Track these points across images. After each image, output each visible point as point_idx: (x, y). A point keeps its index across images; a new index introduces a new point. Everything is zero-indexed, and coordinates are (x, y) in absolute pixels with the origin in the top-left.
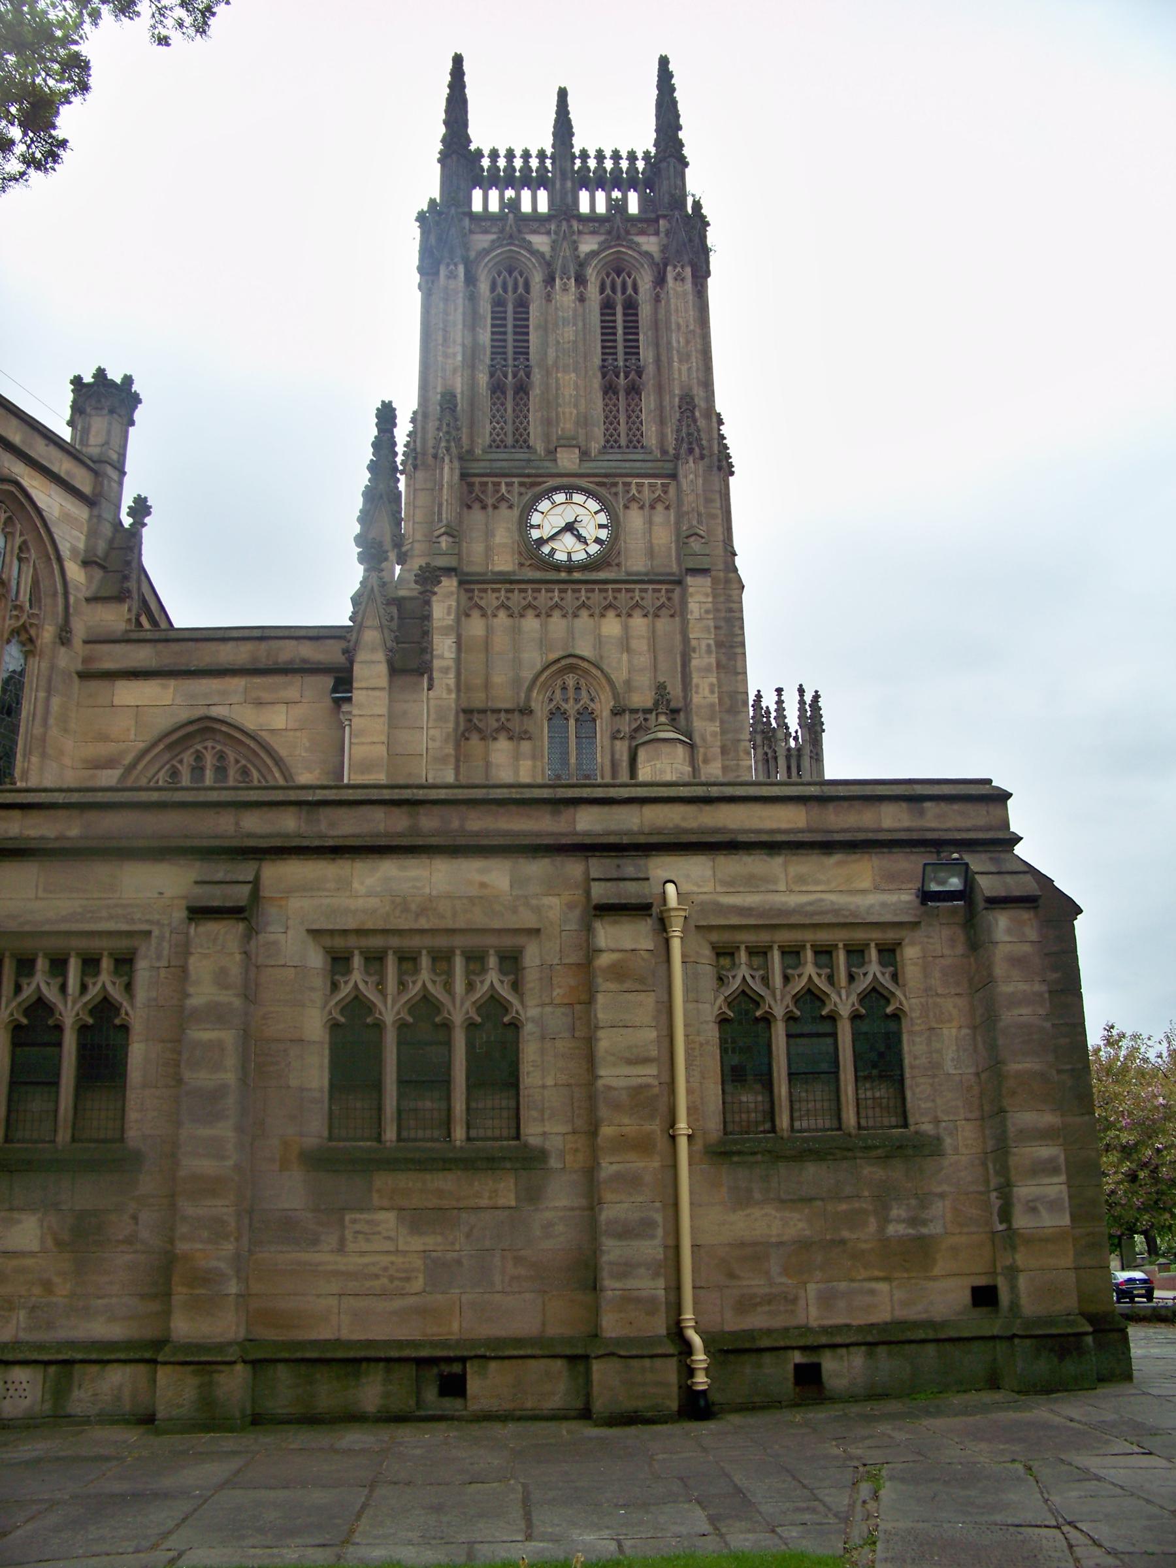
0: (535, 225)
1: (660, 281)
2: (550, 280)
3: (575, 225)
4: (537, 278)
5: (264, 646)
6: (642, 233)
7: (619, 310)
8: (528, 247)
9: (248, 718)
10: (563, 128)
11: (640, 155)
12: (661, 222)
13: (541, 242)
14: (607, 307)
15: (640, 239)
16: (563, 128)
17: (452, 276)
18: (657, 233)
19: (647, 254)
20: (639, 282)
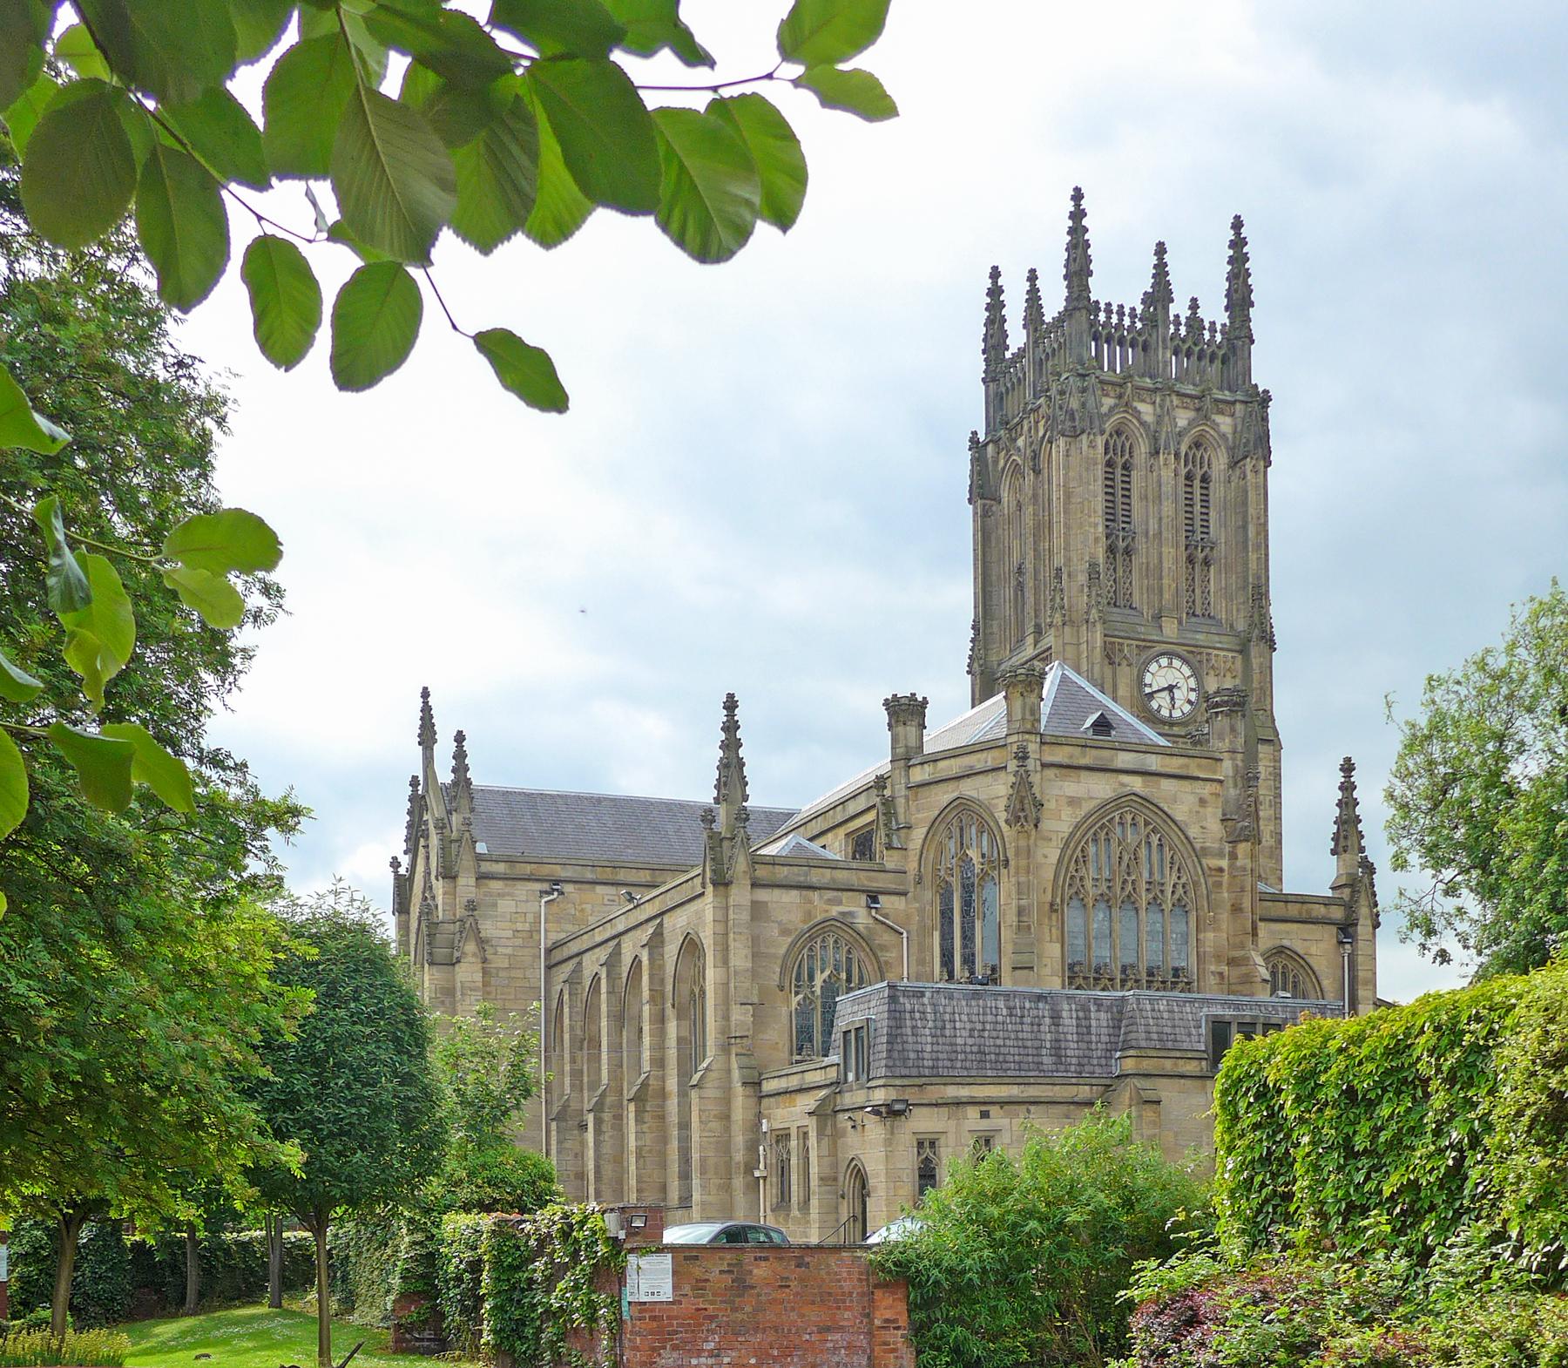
0: (1145, 395)
1: (1234, 464)
2: (1156, 453)
3: (1174, 398)
4: (1143, 448)
5: (1305, 907)
6: (1222, 413)
7: (1197, 483)
8: (1137, 414)
9: (1299, 947)
10: (1160, 293)
11: (1219, 327)
12: (1238, 406)
13: (1145, 409)
14: (1189, 477)
15: (1219, 419)
16: (1160, 293)
17: (1092, 446)
18: (1233, 415)
19: (1223, 436)
20: (1213, 460)
